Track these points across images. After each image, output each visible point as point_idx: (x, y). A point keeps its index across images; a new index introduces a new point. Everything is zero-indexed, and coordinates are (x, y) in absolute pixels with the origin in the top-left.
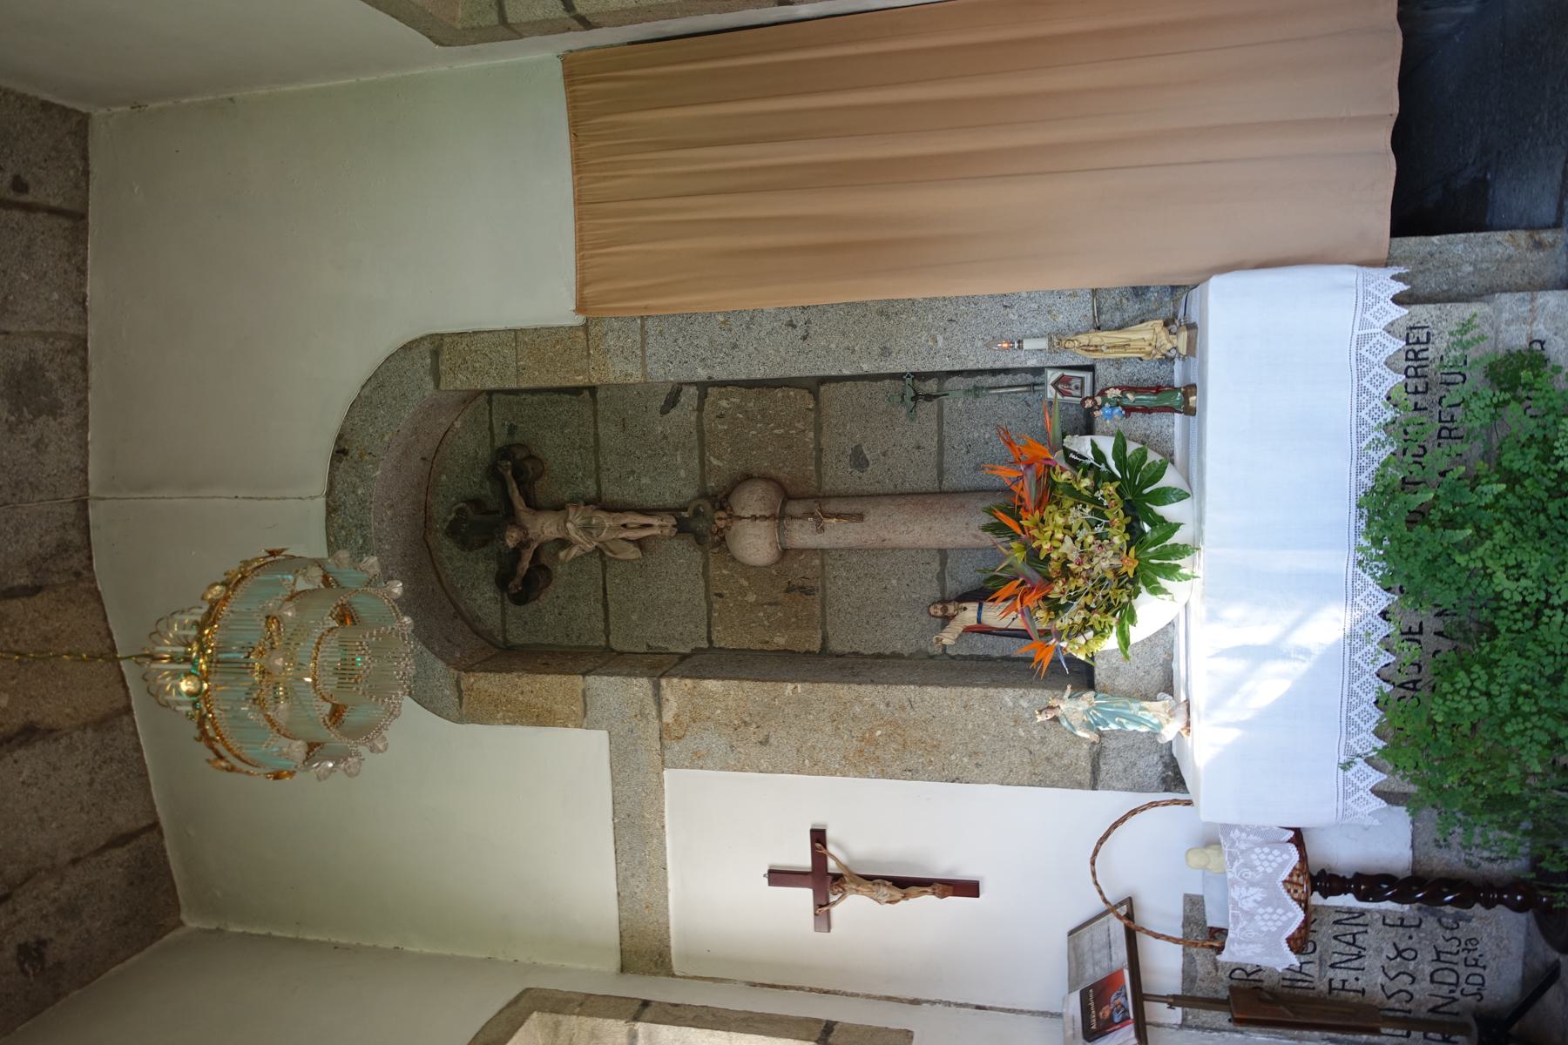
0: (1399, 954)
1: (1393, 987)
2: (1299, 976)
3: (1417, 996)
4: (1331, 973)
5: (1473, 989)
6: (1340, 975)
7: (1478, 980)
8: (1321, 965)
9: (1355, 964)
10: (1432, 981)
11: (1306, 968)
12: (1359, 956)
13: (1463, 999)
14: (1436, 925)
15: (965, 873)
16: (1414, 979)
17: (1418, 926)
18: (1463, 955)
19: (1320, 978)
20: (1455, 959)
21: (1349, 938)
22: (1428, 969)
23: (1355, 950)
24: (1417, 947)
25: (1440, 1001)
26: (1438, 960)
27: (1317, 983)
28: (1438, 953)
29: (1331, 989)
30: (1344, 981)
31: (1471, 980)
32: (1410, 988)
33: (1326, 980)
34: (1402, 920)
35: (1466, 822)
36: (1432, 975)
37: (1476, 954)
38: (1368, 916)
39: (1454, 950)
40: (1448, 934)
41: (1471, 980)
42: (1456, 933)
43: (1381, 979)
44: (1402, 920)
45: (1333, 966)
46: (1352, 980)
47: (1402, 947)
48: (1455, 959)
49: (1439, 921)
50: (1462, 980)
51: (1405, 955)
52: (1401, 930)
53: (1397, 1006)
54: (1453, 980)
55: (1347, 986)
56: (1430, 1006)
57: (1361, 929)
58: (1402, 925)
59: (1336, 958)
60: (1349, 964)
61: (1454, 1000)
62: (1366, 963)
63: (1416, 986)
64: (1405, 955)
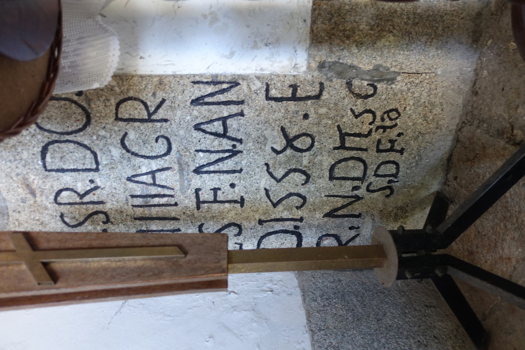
0: (290, 142)
1: (279, 191)
2: (154, 190)
3: (310, 200)
4: (197, 181)
5: (383, 182)
6: (207, 183)
7: (391, 169)
8: (181, 170)
9: (229, 165)
10: (332, 178)
11: (161, 178)
12: (234, 153)
13: (368, 196)
14: (344, 92)
15: (105, 14)
16: (308, 176)
17: (318, 97)
18: (376, 136)
19: (183, 190)
20: (364, 142)
21: (217, 126)
22: (327, 161)
23: (227, 144)
24: (313, 131)
25: (340, 202)
26: (342, 147)
27: (179, 197)
28: (343, 136)
29: (199, 203)
30: (215, 190)
31: (383, 170)
32: (302, 191)
33: (191, 192)
34: (294, 87)
35: (324, 310)
36: (332, 169)
37: (394, 132)
38: (244, 85)
39: (365, 129)
40: (360, 106)
41: (383, 170)
42: (371, 104)
43: (265, 181)
44: (294, 87)
45: (198, 171)
46: (226, 187)
47: (293, 132)
48: (364, 142)
49: (349, 84)
50: (370, 172)
51: (297, 144)
52: (292, 105)
53: (285, 215)
54: (358, 173)
55: (221, 196)
56: (327, 209)
57: (234, 109)
58: (294, 98)
59: (202, 159)
60: (221, 166)
61: (358, 198)
62: (240, 161)
63: (311, 186)
64: (297, 144)
